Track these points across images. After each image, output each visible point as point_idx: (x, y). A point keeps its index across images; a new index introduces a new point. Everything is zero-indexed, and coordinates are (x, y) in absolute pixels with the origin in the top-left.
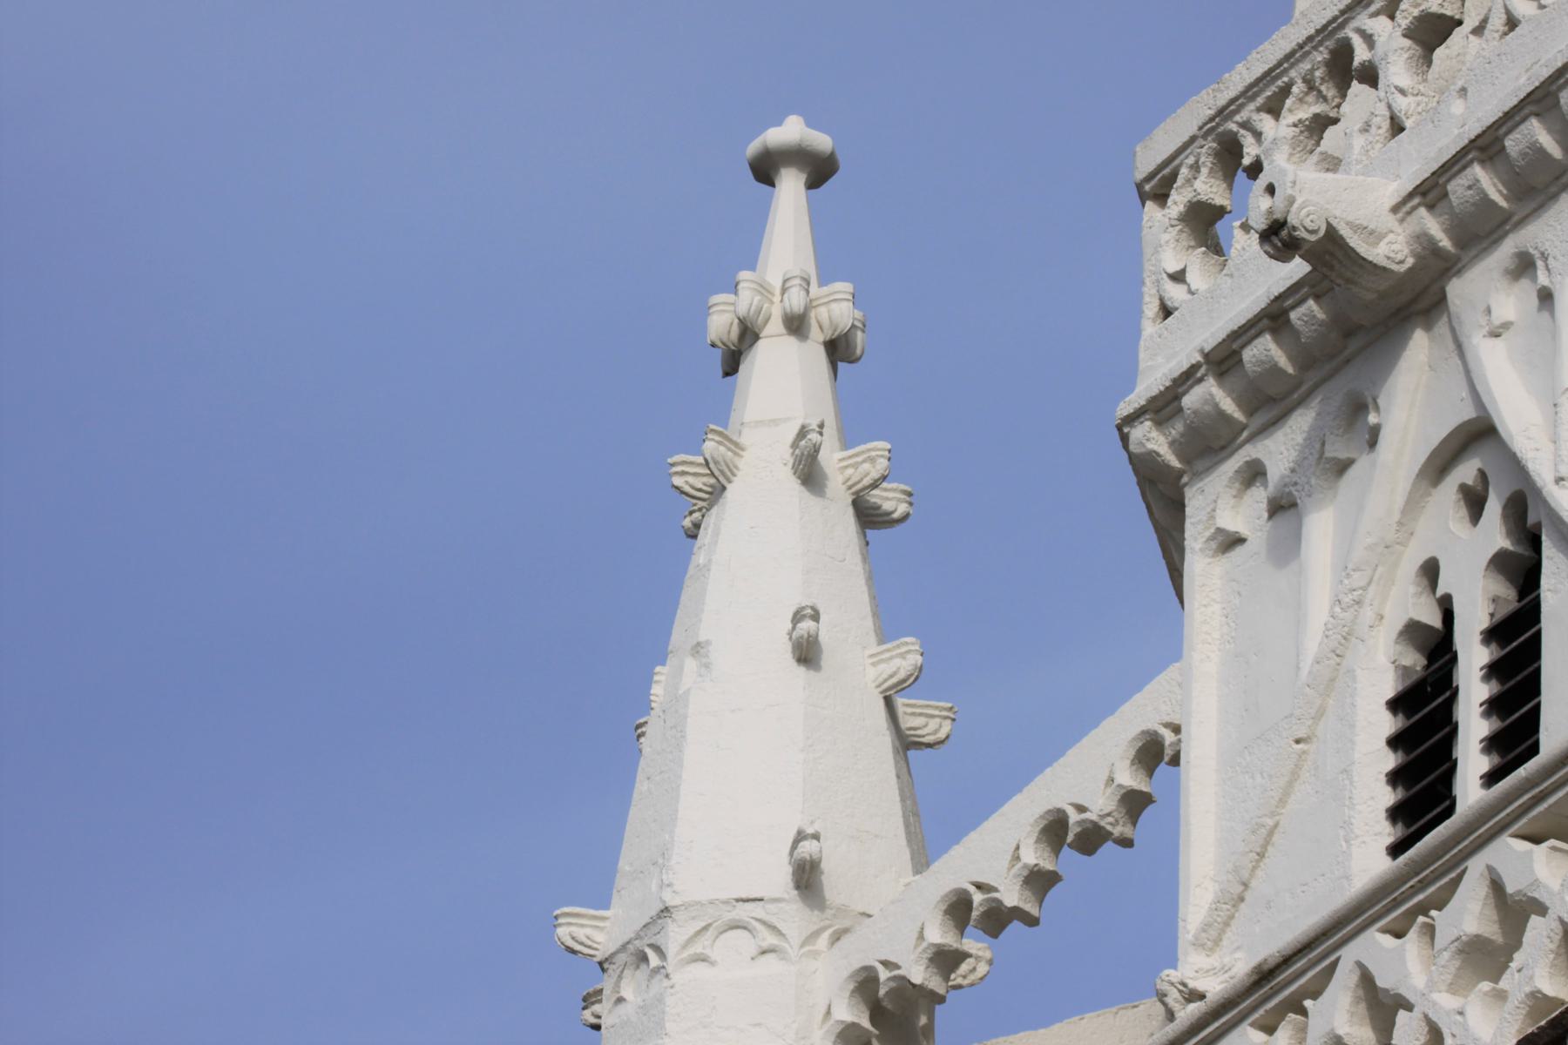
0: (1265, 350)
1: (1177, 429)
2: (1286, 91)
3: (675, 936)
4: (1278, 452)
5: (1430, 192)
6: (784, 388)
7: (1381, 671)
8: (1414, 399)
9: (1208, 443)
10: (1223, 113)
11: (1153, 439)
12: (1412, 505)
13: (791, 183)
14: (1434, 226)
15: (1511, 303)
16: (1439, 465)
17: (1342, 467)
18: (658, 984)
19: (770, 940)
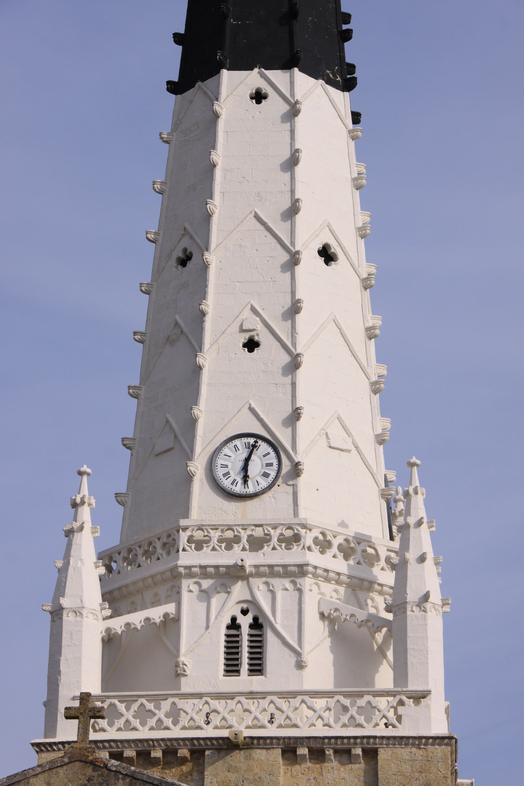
0: (212, 570)
1: (187, 571)
2: (237, 539)
3: (84, 612)
4: (206, 584)
5: (256, 567)
8: (239, 591)
9: (190, 575)
10: (202, 525)
11: (182, 570)
12: (233, 606)
13: (85, 478)
14: (253, 570)
15: (262, 587)
16: (239, 602)
17: (218, 592)
18: (78, 618)
19: (96, 617)
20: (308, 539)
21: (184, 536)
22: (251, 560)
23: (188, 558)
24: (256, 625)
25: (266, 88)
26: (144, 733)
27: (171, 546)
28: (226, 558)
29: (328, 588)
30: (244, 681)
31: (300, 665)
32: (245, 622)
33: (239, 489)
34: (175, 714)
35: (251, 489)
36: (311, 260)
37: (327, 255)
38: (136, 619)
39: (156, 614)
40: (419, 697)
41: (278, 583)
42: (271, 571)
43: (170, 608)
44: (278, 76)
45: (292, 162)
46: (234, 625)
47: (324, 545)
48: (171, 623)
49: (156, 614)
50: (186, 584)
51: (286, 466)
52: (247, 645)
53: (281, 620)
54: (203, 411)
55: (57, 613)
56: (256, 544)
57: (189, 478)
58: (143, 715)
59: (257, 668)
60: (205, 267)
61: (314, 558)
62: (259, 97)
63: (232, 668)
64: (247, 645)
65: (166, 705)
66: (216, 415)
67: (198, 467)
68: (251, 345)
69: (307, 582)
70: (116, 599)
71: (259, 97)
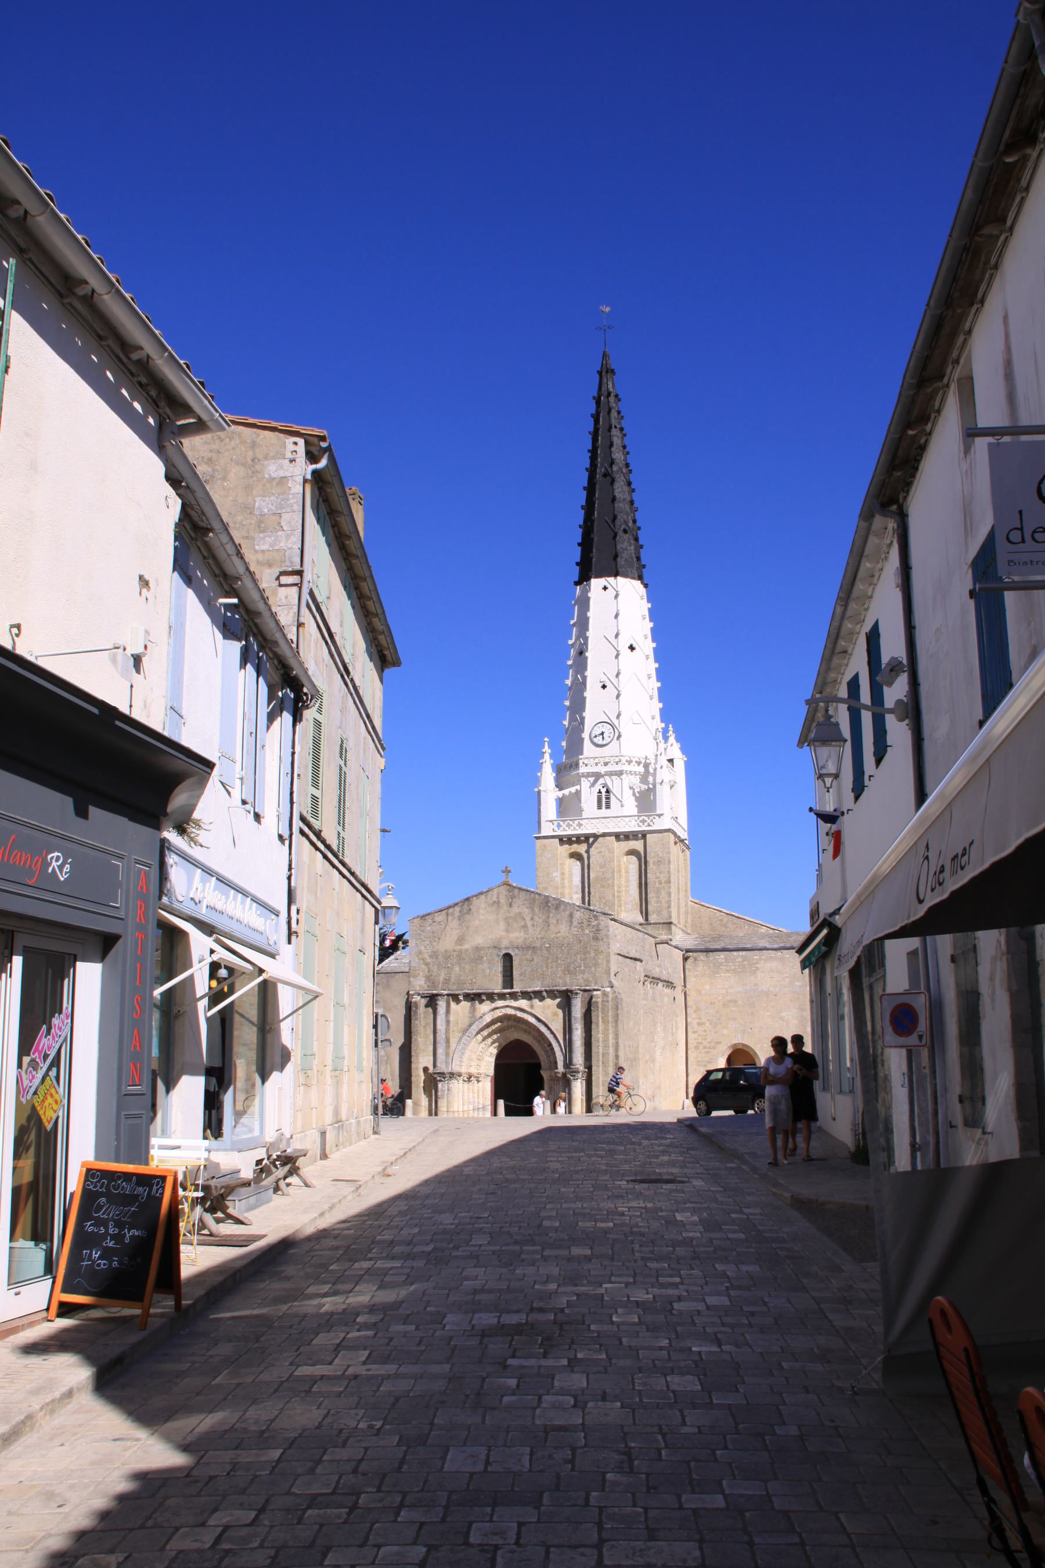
6: (547, 756)
7: (596, 794)
8: (601, 781)
20: (624, 760)
21: (581, 762)
22: (602, 769)
23: (582, 770)
24: (608, 791)
25: (608, 585)
26: (569, 832)
27: (577, 765)
28: (595, 769)
29: (632, 777)
30: (604, 812)
31: (622, 806)
32: (604, 790)
33: (600, 742)
34: (580, 825)
35: (604, 742)
36: (625, 651)
37: (632, 648)
38: (566, 792)
39: (573, 789)
40: (660, 816)
41: (614, 777)
42: (610, 774)
43: (578, 787)
44: (611, 580)
45: (616, 616)
46: (600, 792)
47: (630, 762)
48: (578, 793)
49: (573, 789)
50: (583, 779)
51: (617, 734)
52: (605, 799)
53: (615, 790)
54: (587, 714)
55: (539, 792)
56: (606, 764)
57: (583, 740)
58: (569, 826)
59: (608, 807)
60: (586, 658)
61: (626, 767)
62: (605, 588)
63: (599, 807)
64: (605, 799)
65: (576, 822)
66: (591, 715)
67: (585, 735)
68: (604, 687)
69: (624, 776)
70: (560, 786)
71: (605, 588)
